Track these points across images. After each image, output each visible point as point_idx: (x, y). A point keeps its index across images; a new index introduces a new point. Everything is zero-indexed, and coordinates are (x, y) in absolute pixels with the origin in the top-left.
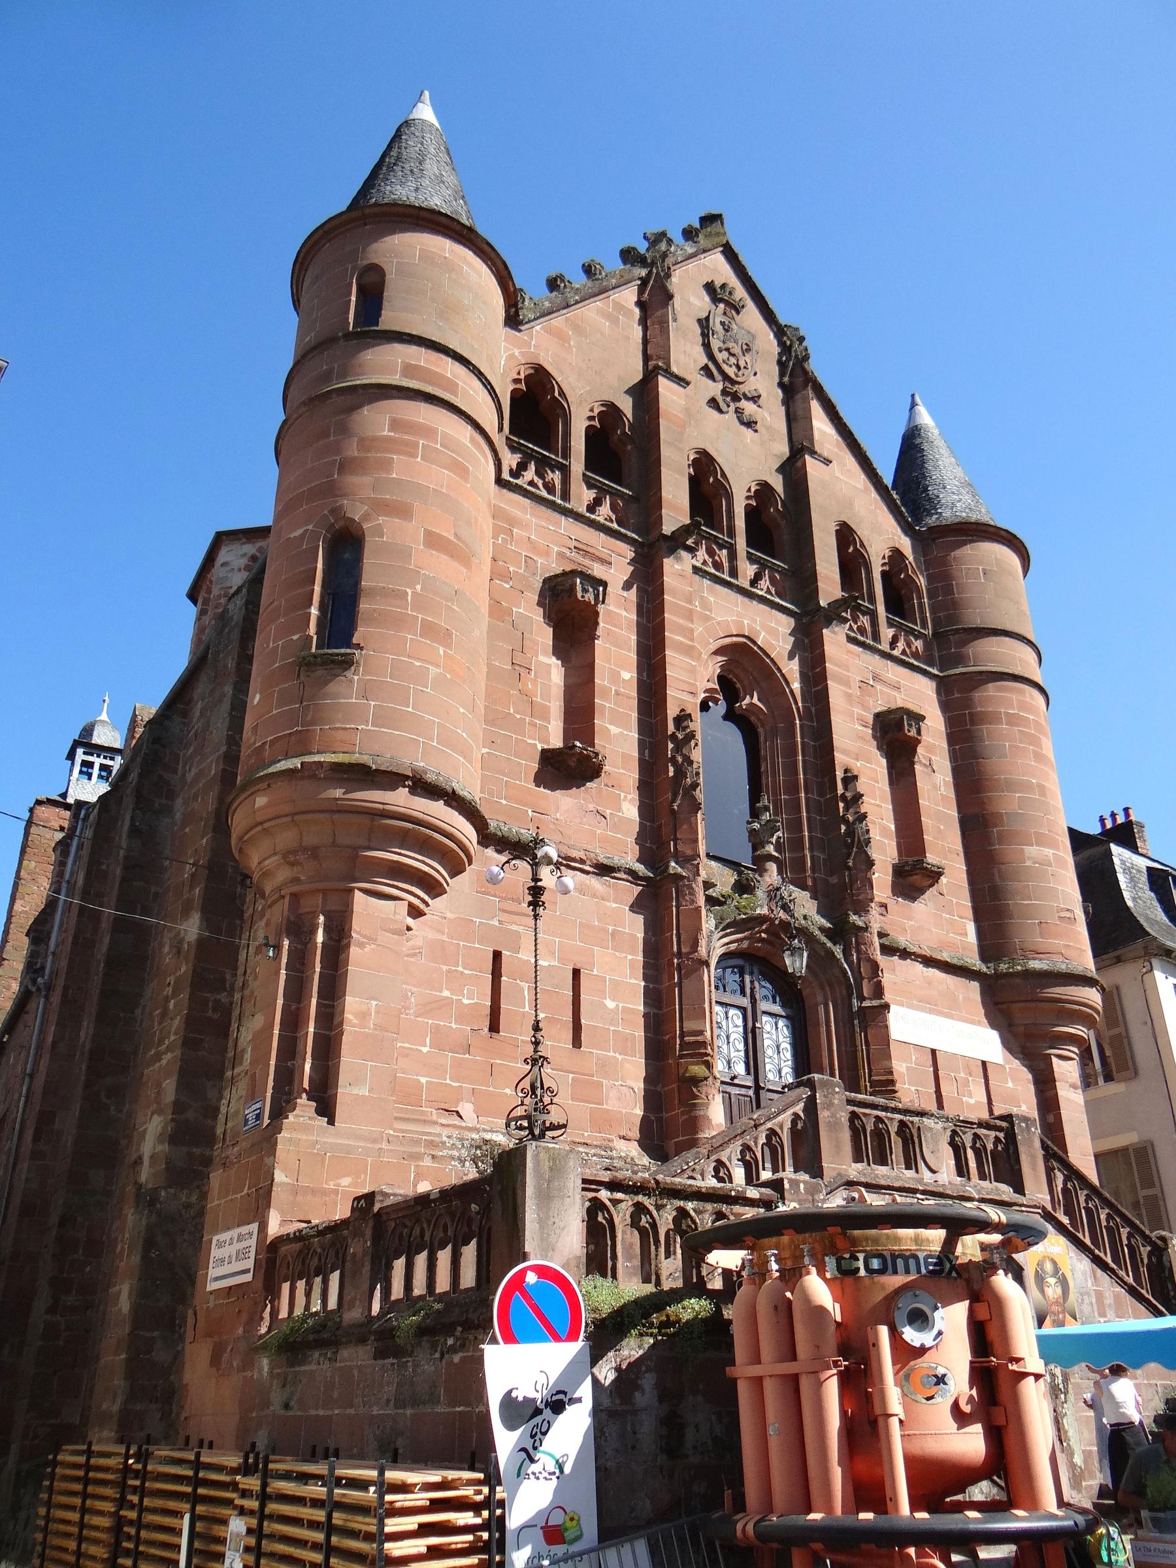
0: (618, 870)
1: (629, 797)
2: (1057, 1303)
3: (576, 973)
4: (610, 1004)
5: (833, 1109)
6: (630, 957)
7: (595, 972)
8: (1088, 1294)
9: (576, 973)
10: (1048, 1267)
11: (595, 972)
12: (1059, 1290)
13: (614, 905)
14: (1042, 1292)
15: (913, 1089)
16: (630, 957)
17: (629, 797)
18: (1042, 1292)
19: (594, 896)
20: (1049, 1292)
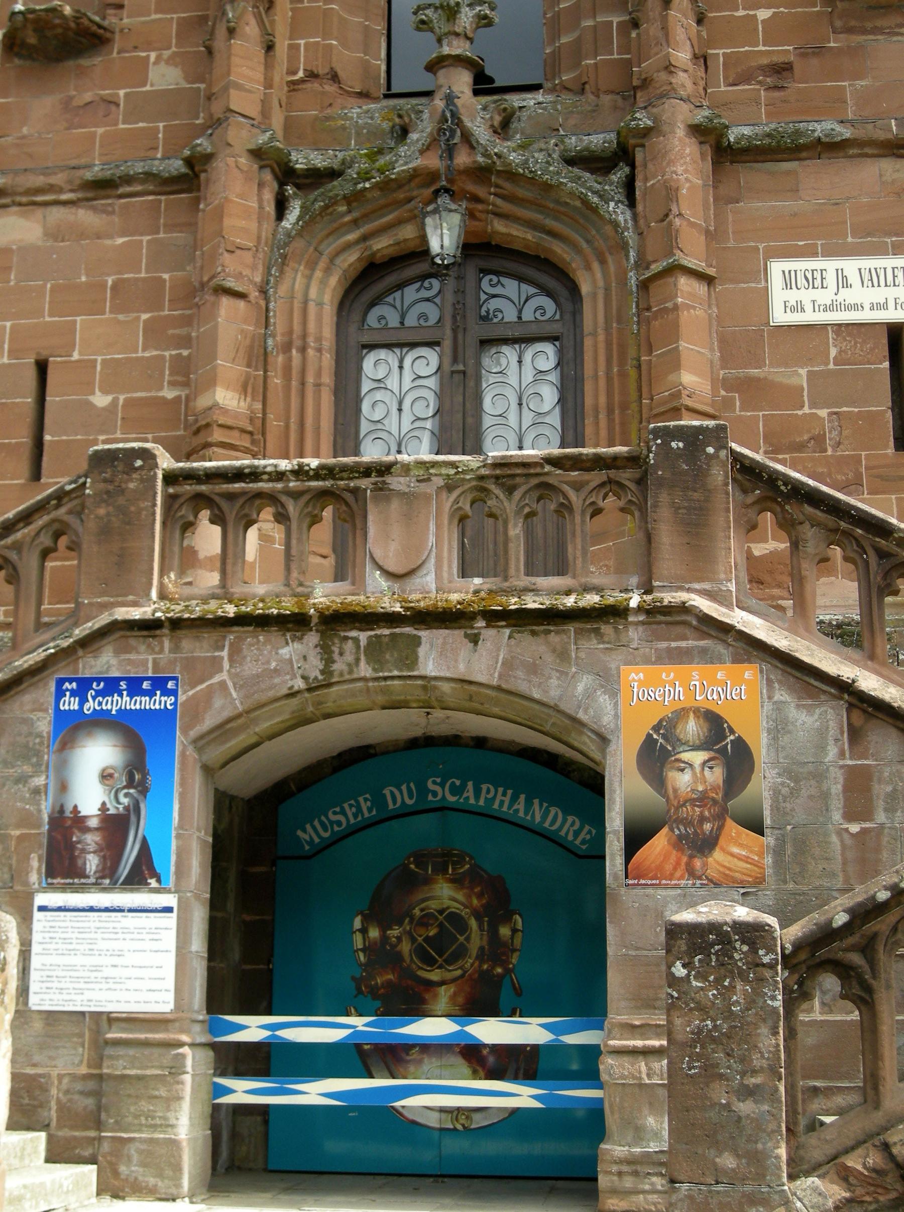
0: (128, 179)
1: (166, 54)
2: (702, 799)
3: (42, 368)
4: (101, 400)
5: (121, 501)
6: (145, 316)
7: (76, 356)
8: (819, 776)
9: (42, 368)
10: (692, 728)
11: (76, 356)
12: (716, 776)
13: (120, 241)
14: (658, 781)
15: (823, 413)
16: (145, 316)
17: (166, 54)
18: (658, 781)
19: (82, 235)
20: (682, 781)
